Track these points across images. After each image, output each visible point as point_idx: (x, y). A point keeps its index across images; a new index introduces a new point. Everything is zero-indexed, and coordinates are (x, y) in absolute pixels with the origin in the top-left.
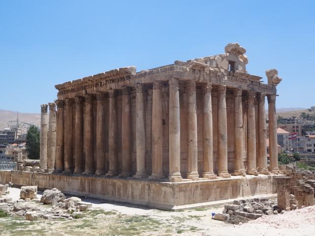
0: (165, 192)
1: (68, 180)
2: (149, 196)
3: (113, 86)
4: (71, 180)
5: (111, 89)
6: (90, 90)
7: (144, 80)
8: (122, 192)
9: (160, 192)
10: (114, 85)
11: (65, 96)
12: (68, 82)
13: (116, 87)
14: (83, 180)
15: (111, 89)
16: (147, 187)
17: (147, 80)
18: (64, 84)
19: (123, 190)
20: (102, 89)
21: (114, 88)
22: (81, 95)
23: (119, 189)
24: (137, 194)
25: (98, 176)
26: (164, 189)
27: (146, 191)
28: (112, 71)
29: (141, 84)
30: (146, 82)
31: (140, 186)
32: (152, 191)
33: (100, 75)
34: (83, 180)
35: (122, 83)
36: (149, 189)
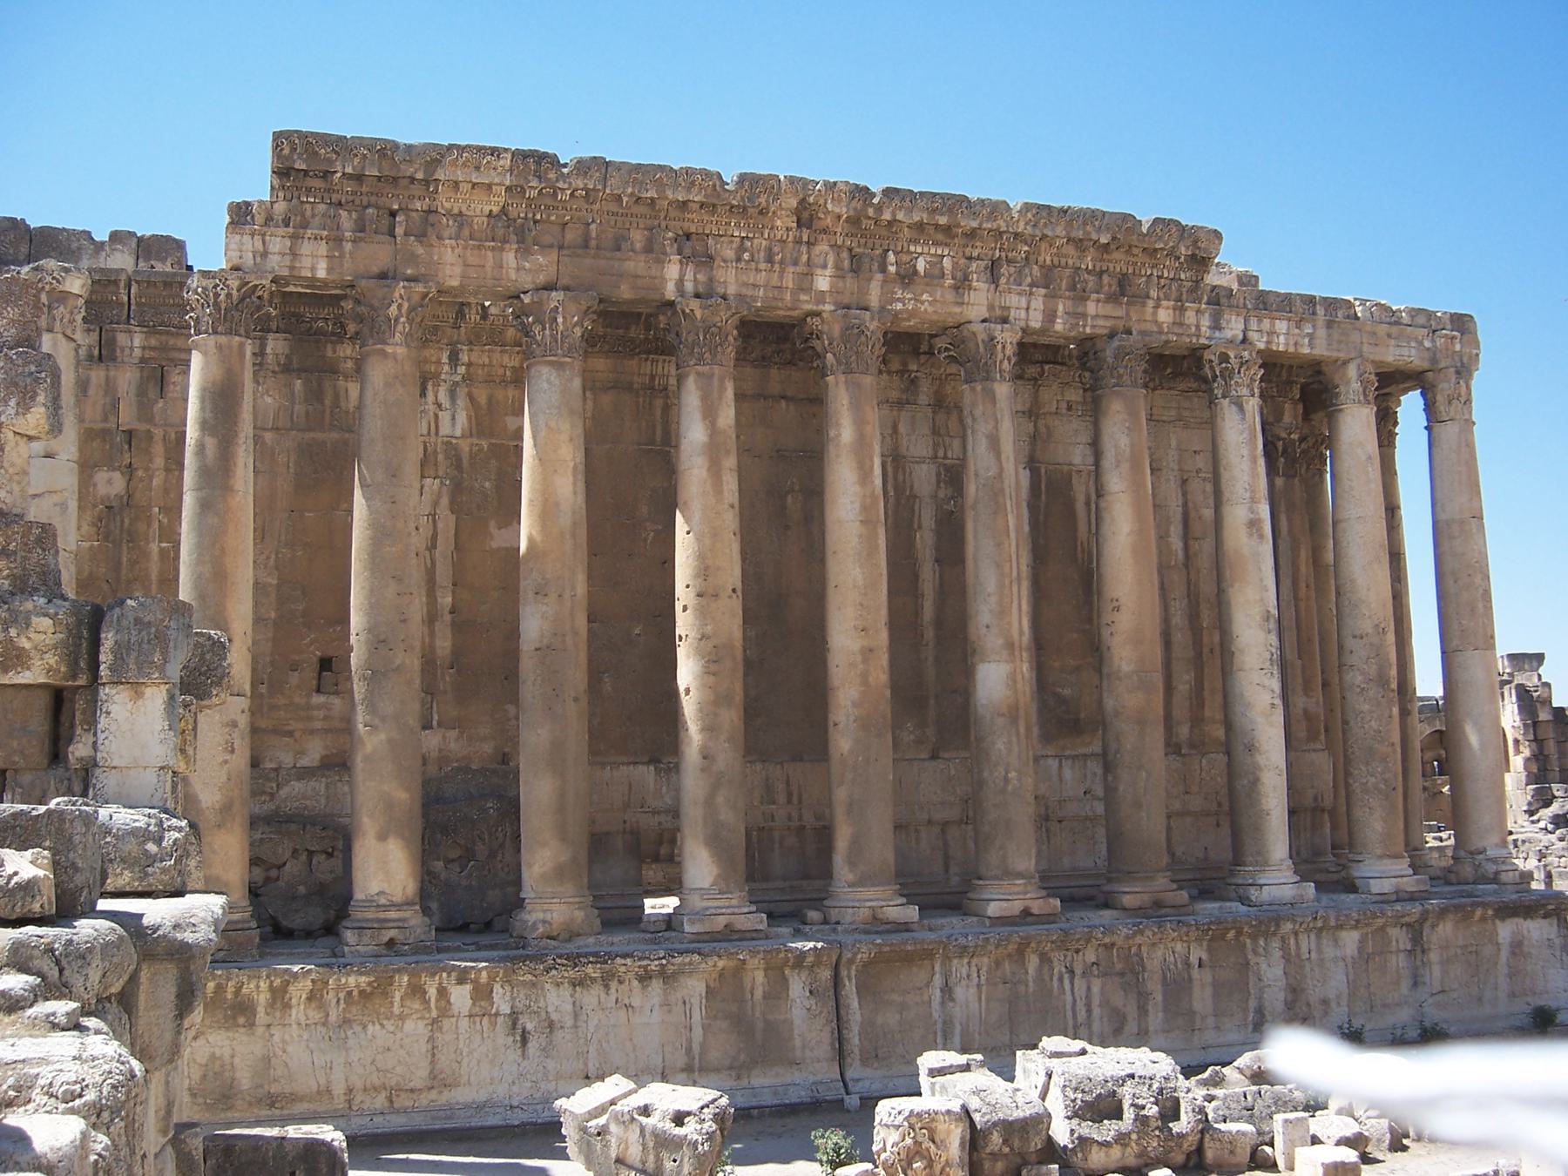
0: (1517, 946)
1: (502, 1000)
2: (1415, 984)
3: (1029, 310)
4: (557, 999)
5: (1005, 321)
6: (762, 278)
7: (1282, 336)
8: (1201, 999)
9: (1487, 950)
10: (1038, 303)
11: (378, 254)
12: (522, 156)
13: (1050, 316)
14: (757, 977)
15: (1005, 321)
16: (1399, 937)
17: (1311, 336)
18: (436, 155)
19: (1217, 985)
20: (923, 307)
21: (1036, 324)
22: (625, 292)
23: (1177, 987)
24: (1332, 995)
25: (904, 927)
26: (1505, 931)
27: (1399, 962)
28: (1092, 217)
29: (1259, 352)
30: (1306, 350)
31: (1350, 939)
32: (1434, 956)
33: (957, 203)
34: (757, 977)
35: (1120, 312)
36: (1418, 944)
